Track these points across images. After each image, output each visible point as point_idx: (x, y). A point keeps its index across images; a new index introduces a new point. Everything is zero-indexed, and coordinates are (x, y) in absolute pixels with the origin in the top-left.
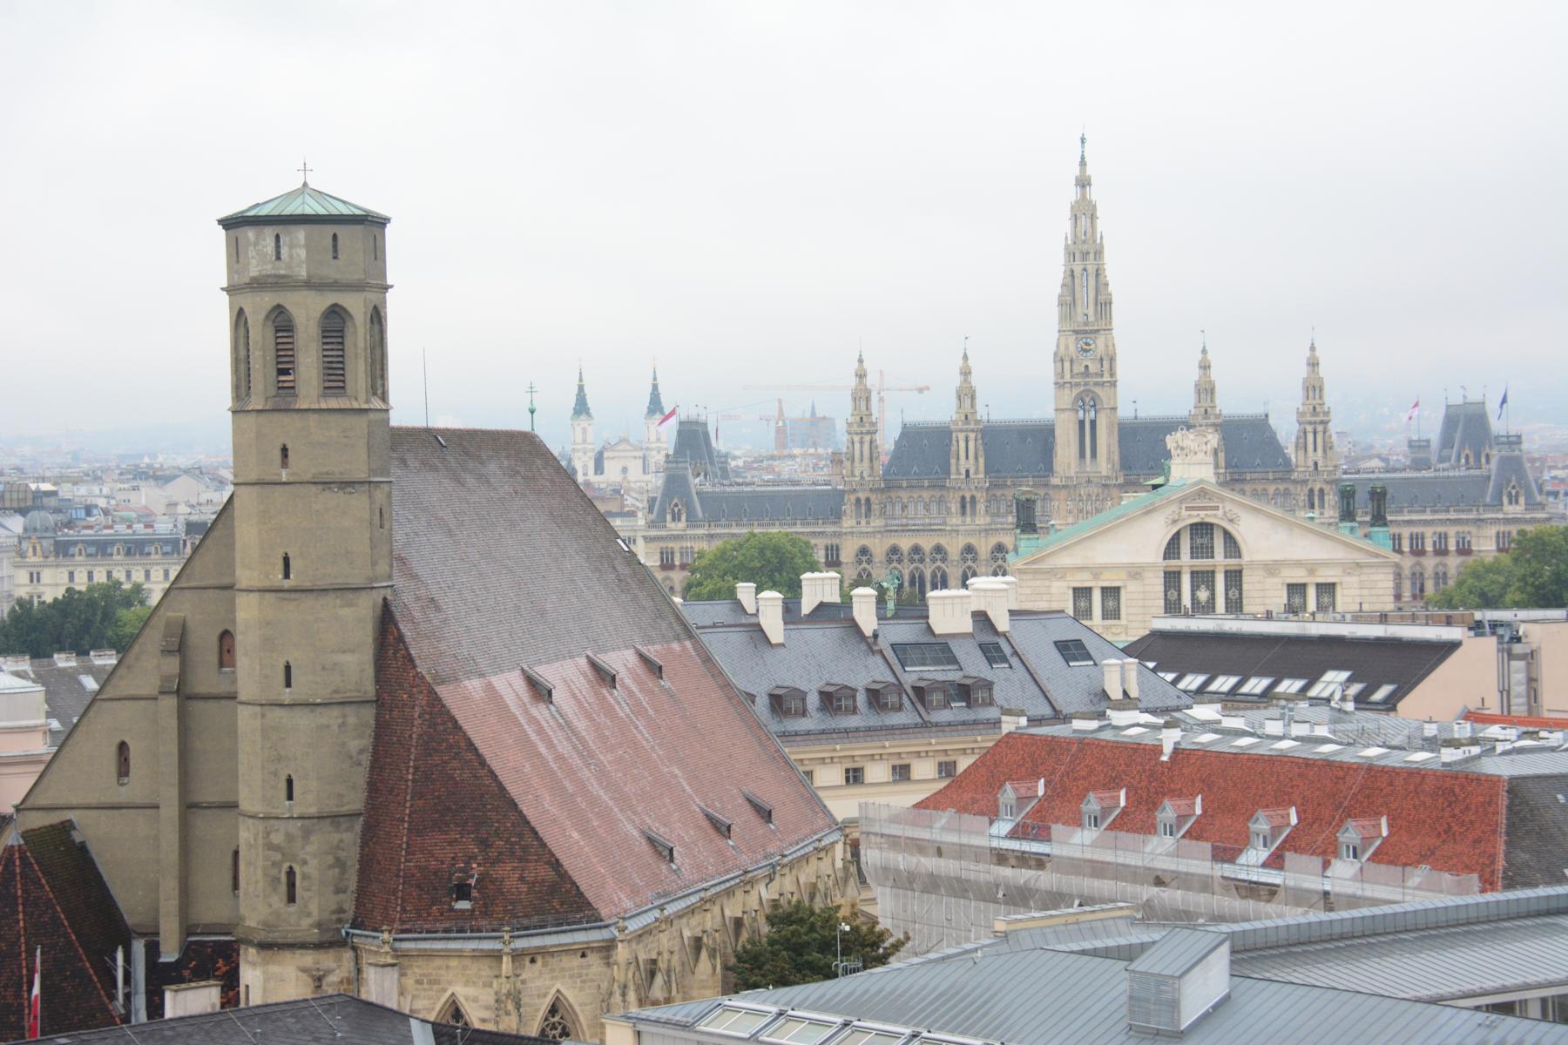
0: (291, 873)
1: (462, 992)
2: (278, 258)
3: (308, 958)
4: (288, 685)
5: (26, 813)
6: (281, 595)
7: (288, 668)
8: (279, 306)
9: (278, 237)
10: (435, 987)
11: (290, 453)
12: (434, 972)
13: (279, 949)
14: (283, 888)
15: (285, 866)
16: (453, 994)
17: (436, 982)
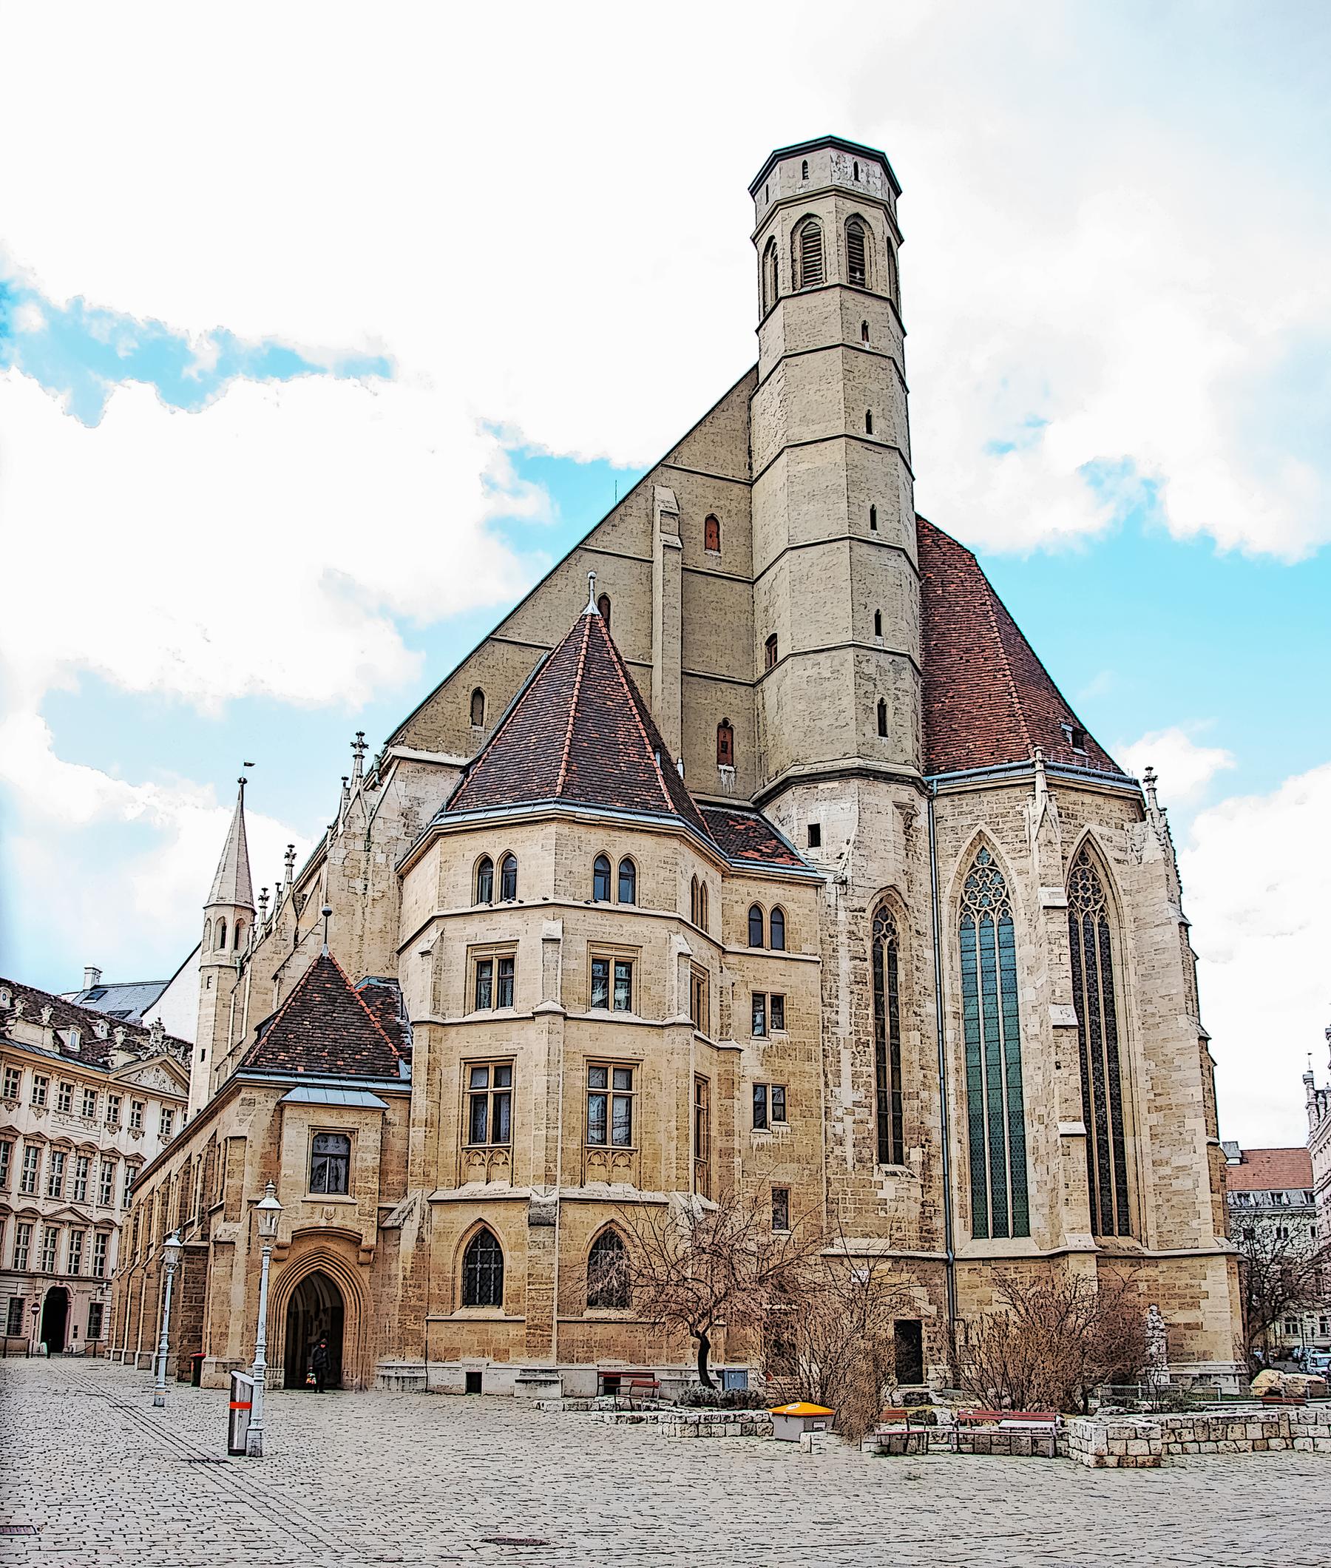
0: (882, 707)
1: (1096, 829)
2: (856, 178)
3: (906, 794)
4: (874, 527)
5: (496, 643)
6: (867, 445)
7: (873, 513)
8: (857, 215)
9: (856, 165)
10: (1072, 822)
11: (870, 331)
12: (1071, 806)
13: (876, 778)
14: (875, 718)
15: (878, 698)
16: (1089, 831)
17: (1074, 817)
